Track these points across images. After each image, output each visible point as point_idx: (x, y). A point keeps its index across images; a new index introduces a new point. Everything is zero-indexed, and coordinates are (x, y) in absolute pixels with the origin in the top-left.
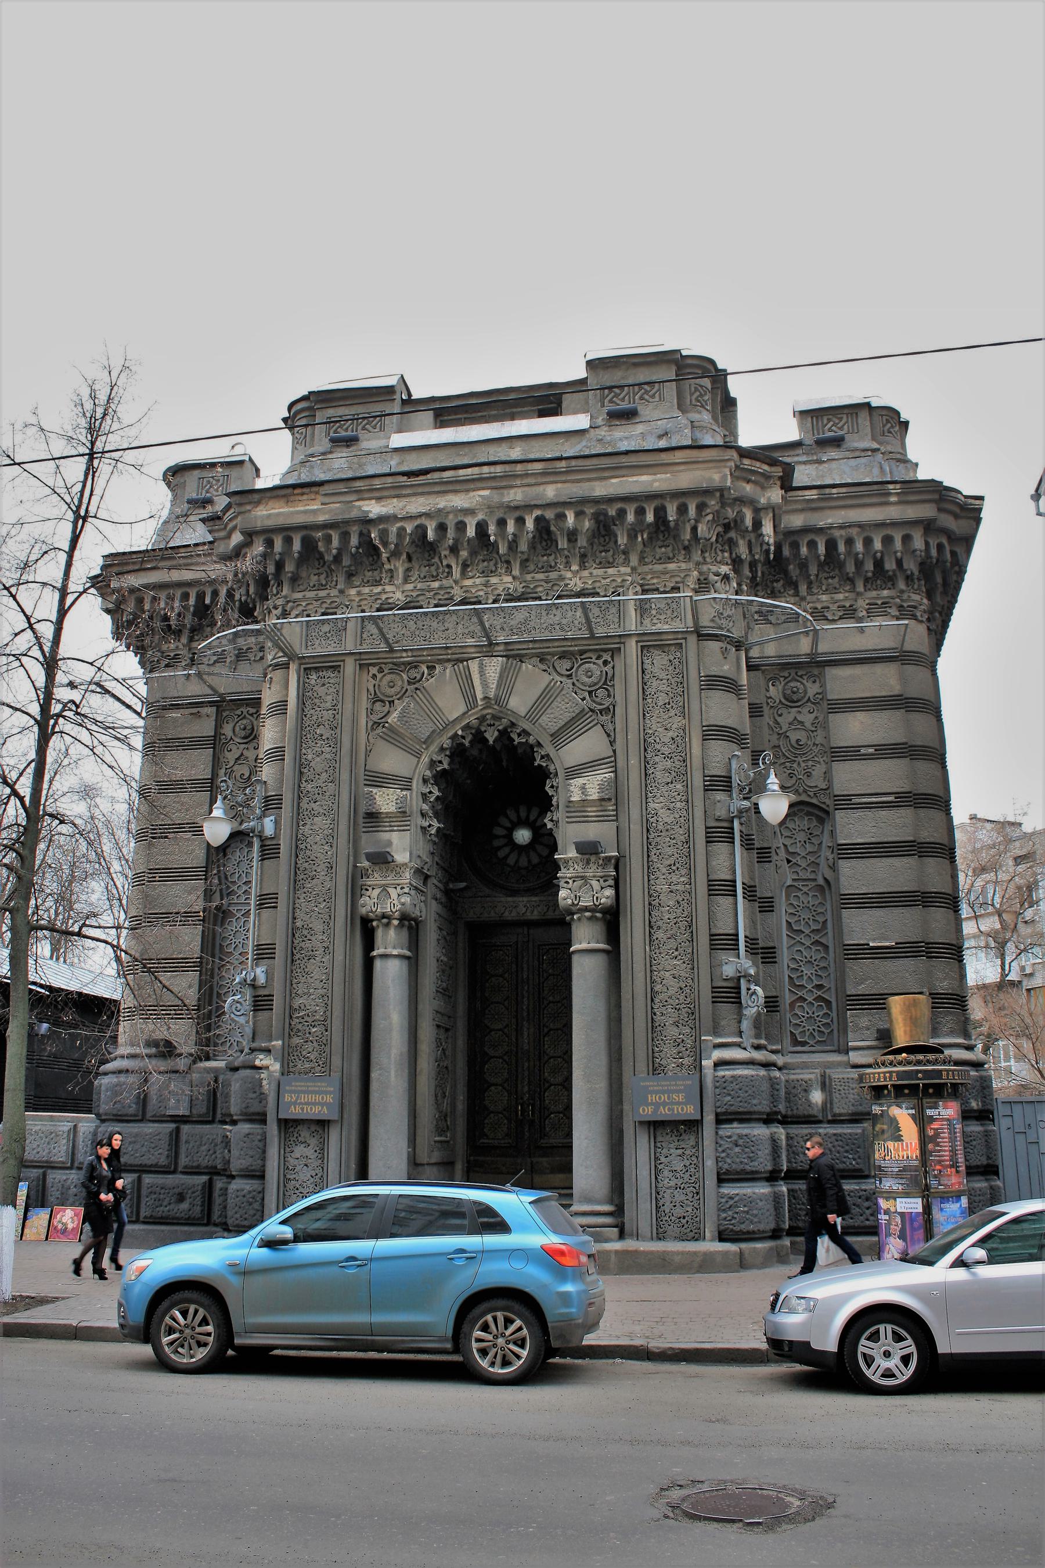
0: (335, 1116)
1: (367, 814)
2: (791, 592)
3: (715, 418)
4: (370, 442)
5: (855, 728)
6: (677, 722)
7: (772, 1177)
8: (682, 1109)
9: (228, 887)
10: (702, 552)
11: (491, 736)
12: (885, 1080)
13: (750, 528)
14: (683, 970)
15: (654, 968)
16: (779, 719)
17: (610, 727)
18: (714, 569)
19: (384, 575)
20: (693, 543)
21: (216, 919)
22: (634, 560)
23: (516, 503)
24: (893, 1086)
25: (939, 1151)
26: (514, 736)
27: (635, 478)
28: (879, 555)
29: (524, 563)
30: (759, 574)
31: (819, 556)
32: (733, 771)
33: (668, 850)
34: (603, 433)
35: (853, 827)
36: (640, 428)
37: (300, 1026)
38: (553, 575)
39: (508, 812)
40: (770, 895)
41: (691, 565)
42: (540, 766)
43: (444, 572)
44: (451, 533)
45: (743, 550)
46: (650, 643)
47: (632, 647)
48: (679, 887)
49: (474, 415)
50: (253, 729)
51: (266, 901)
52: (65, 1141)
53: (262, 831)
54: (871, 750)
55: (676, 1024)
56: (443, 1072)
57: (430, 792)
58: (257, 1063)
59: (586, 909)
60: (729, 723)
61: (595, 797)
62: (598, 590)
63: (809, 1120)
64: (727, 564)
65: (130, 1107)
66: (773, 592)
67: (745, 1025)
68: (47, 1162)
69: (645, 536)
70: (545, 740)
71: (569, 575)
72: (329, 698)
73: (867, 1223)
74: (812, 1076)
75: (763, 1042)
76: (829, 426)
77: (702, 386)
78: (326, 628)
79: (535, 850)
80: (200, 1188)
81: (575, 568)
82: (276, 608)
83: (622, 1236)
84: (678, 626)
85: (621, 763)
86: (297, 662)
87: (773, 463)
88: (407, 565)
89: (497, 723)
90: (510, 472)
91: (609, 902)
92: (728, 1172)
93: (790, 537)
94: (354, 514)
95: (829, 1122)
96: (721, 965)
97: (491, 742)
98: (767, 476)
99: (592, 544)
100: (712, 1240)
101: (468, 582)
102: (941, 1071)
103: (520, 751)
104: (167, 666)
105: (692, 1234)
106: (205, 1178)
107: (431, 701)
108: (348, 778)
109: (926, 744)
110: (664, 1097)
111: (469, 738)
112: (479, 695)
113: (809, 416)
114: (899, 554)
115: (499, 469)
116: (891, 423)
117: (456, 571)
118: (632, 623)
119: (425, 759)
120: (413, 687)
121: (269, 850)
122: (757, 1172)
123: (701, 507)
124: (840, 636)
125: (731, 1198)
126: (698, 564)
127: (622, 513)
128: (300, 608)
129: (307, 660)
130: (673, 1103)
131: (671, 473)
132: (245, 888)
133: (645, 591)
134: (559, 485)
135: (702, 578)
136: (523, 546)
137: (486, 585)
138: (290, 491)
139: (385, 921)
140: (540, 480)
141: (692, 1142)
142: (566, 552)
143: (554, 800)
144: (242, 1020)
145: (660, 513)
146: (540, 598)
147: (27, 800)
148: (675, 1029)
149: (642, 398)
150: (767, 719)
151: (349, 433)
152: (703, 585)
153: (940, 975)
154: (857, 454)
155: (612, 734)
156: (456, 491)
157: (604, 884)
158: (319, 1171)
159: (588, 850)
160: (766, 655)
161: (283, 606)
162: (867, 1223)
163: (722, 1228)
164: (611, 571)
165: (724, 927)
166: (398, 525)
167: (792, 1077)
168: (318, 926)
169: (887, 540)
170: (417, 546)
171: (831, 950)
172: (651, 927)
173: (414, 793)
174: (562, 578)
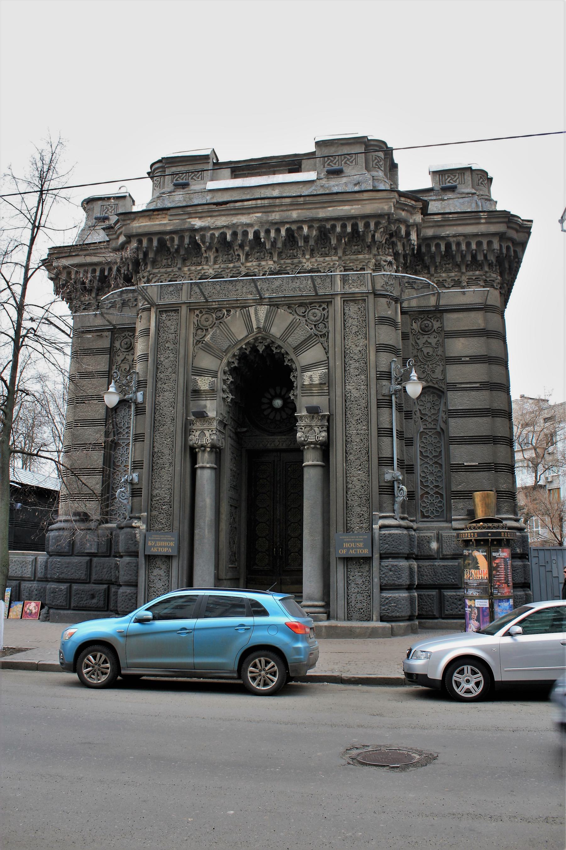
0: (175, 553)
1: (193, 390)
2: (426, 272)
3: (386, 175)
4: (195, 186)
5: (459, 347)
6: (362, 342)
7: (409, 588)
8: (362, 551)
9: (118, 430)
10: (378, 249)
11: (261, 349)
12: (471, 537)
13: (404, 236)
14: (363, 476)
15: (348, 475)
16: (418, 341)
17: (326, 344)
18: (384, 258)
19: (203, 260)
20: (373, 244)
21: (111, 447)
22: (340, 253)
23: (275, 221)
24: (475, 540)
25: (499, 575)
26: (274, 349)
27: (341, 208)
28: (474, 252)
29: (280, 254)
30: (409, 261)
31: (441, 252)
32: (392, 369)
33: (356, 411)
34: (324, 182)
35: (457, 400)
36: (344, 180)
37: (156, 505)
38: (296, 261)
39: (270, 390)
40: (411, 437)
41: (371, 256)
42: (287, 365)
43: (236, 258)
44: (240, 237)
45: (400, 248)
46: (348, 299)
47: (338, 301)
48: (362, 432)
49: (253, 172)
50: (131, 344)
51: (138, 438)
52: (30, 566)
53: (136, 399)
54: (468, 359)
55: (359, 506)
56: (233, 529)
57: (228, 379)
58: (134, 525)
59: (311, 443)
60: (390, 343)
61: (317, 382)
62: (320, 269)
63: (430, 558)
64: (391, 256)
65: (65, 548)
66: (416, 271)
67: (397, 506)
68: (21, 577)
69: (346, 240)
70: (290, 351)
71: (304, 261)
72: (173, 327)
73: (460, 613)
74: (432, 534)
75: (406, 515)
76: (449, 180)
77: (379, 157)
78: (171, 289)
80: (103, 591)
81: (307, 257)
82: (144, 277)
83: (328, 618)
84: (363, 289)
85: (331, 365)
86: (155, 307)
87: (417, 200)
88: (215, 255)
89: (264, 342)
90: (272, 203)
91: (324, 439)
92: (386, 585)
93: (425, 241)
94: (187, 226)
95: (441, 559)
96: (384, 474)
97: (261, 352)
98: (413, 207)
99: (317, 244)
100: (377, 621)
101: (249, 264)
102: (500, 532)
103: (276, 357)
104: (84, 309)
105: (366, 618)
106: (105, 586)
107: (229, 329)
108: (183, 371)
109: (497, 356)
110: (353, 545)
111: (249, 349)
112: (255, 326)
113: (438, 174)
114: (485, 252)
115: (266, 202)
116: (483, 178)
117: (243, 258)
118: (338, 287)
119: (225, 361)
120: (218, 321)
121: (140, 410)
122: (401, 585)
123: (377, 224)
124: (452, 296)
125: (387, 599)
126: (375, 255)
127: (334, 227)
128: (157, 278)
129: (161, 306)
130: (357, 548)
131: (361, 205)
132: (127, 430)
133: (345, 270)
134: (300, 211)
135: (377, 263)
136: (279, 245)
137: (259, 265)
138: (151, 213)
139: (203, 448)
140: (289, 208)
141: (367, 569)
142: (303, 248)
143: (295, 384)
144: (125, 502)
145: (355, 227)
146: (288, 273)
147: (8, 382)
148: (359, 508)
149: (345, 163)
150: (411, 341)
151: (184, 181)
152: (378, 267)
153: (502, 481)
154: (464, 196)
155: (327, 348)
156: (243, 214)
158: (167, 582)
159: (313, 411)
160: (411, 306)
161: (148, 277)
162: (460, 613)
163: (382, 614)
164: (327, 259)
165: (386, 453)
166: (211, 232)
167: (422, 534)
168: (166, 451)
169: (479, 244)
170: (221, 244)
171: (444, 466)
172: (346, 453)
173: (219, 380)
174: (300, 262)
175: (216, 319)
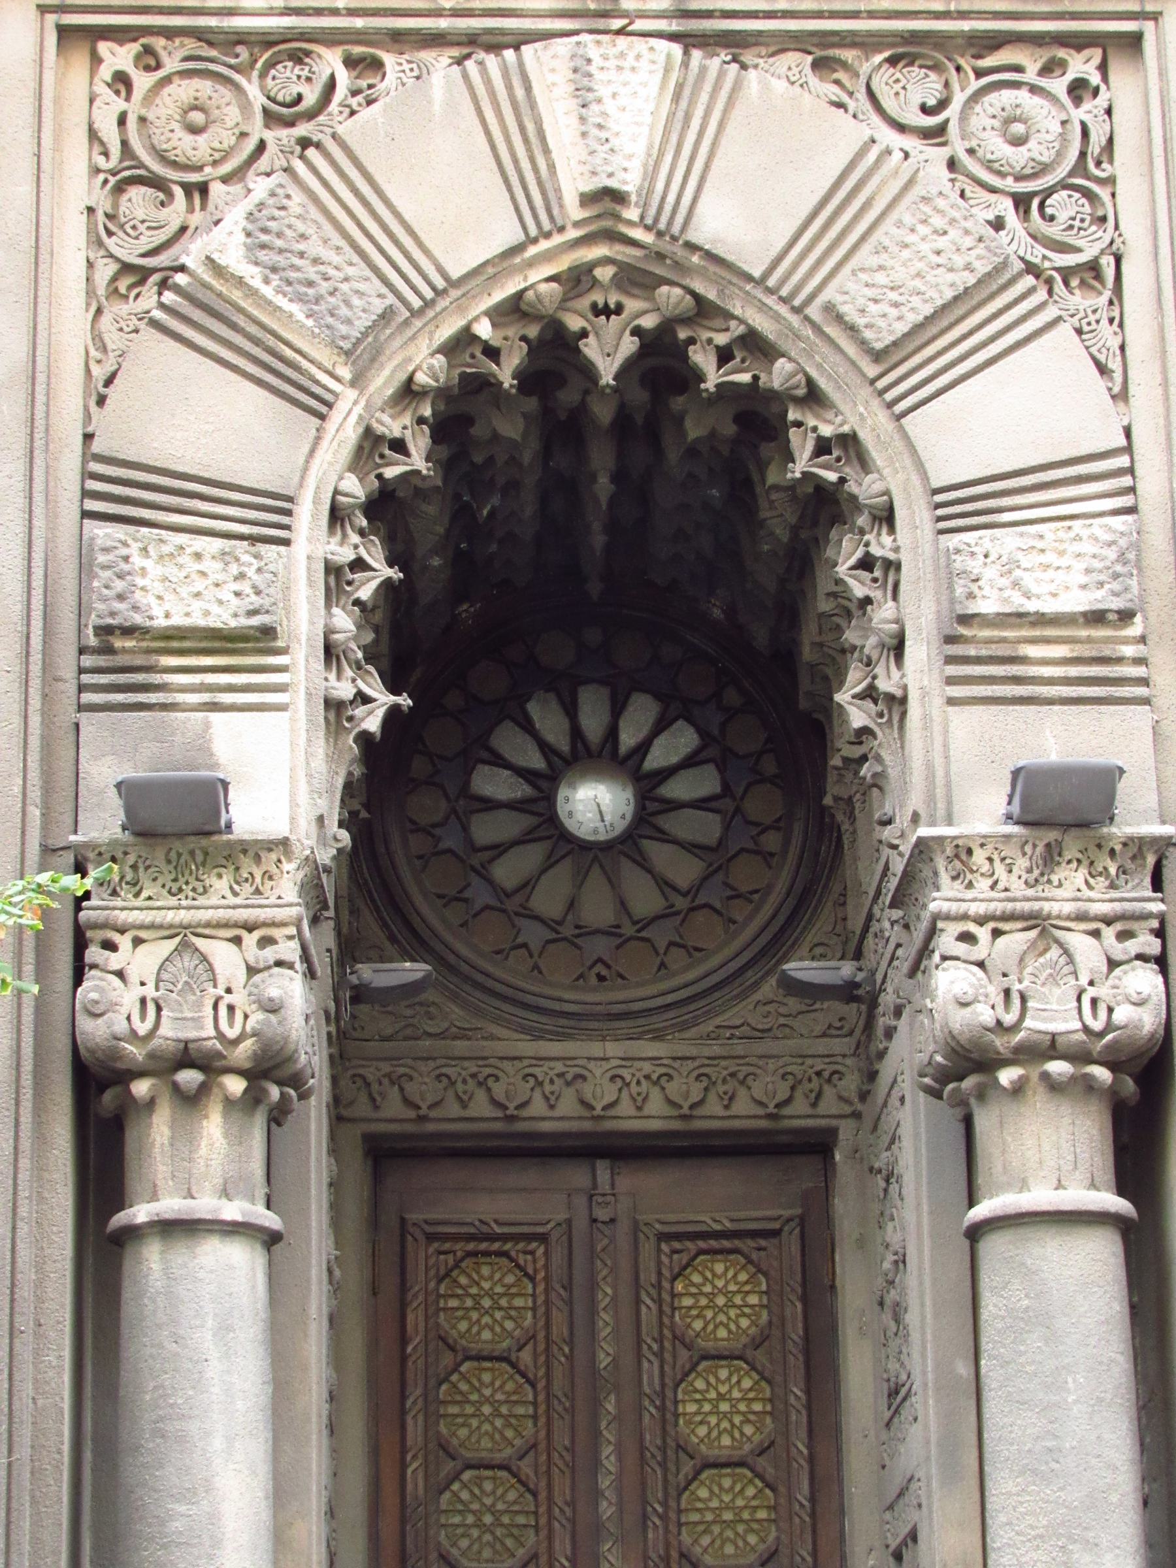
11: (608, 353)
17: (1108, 336)
26: (703, 359)
39: (534, 709)
57: (359, 565)
59: (1051, 1048)
79: (643, 863)
119: (344, 428)
139: (189, 1077)
143: (883, 614)
155: (1115, 365)
157: (1120, 950)
175: (270, 118)
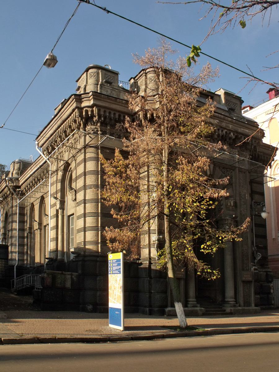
27: (245, 130)
127: (241, 137)
134: (232, 126)
164: (234, 150)
